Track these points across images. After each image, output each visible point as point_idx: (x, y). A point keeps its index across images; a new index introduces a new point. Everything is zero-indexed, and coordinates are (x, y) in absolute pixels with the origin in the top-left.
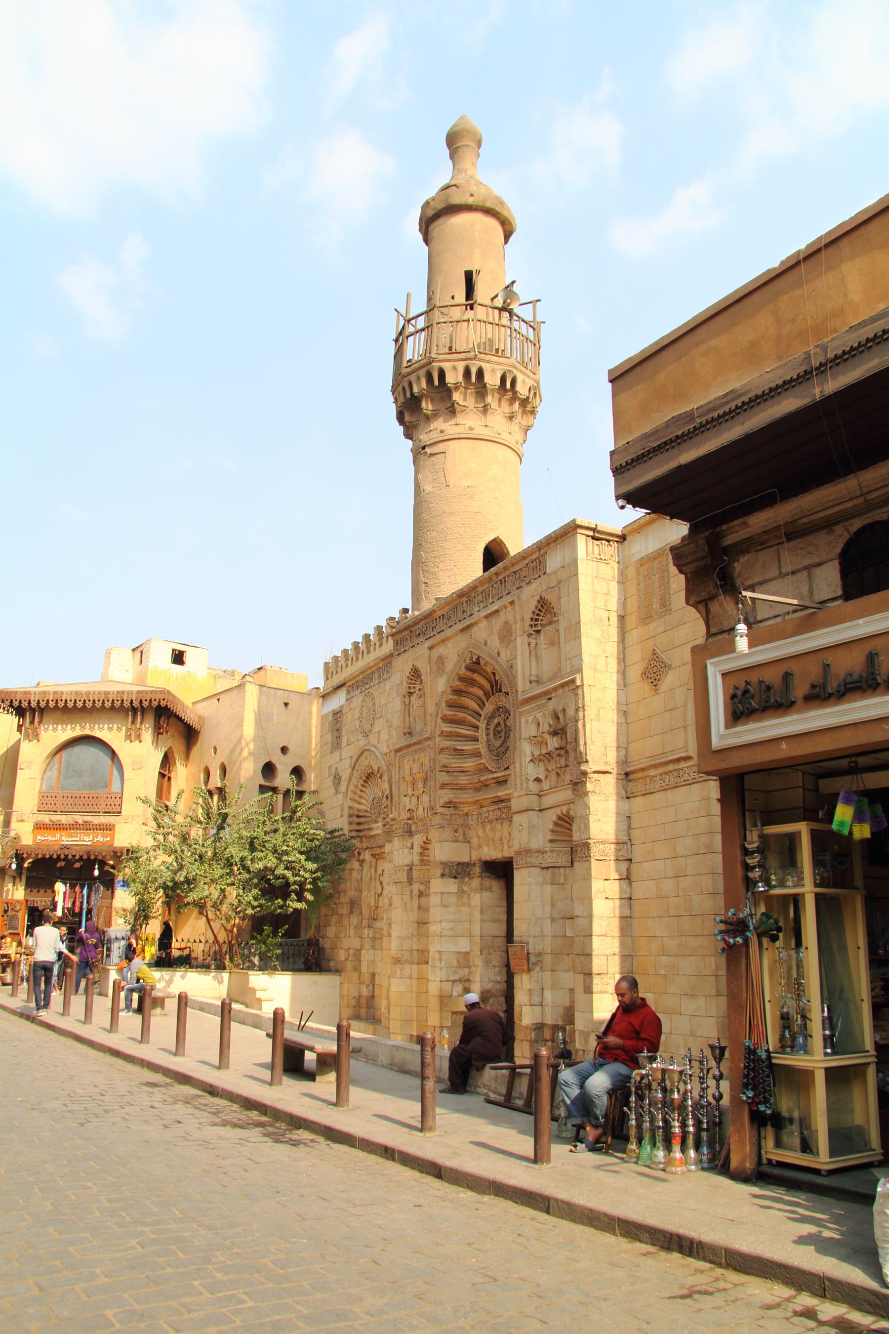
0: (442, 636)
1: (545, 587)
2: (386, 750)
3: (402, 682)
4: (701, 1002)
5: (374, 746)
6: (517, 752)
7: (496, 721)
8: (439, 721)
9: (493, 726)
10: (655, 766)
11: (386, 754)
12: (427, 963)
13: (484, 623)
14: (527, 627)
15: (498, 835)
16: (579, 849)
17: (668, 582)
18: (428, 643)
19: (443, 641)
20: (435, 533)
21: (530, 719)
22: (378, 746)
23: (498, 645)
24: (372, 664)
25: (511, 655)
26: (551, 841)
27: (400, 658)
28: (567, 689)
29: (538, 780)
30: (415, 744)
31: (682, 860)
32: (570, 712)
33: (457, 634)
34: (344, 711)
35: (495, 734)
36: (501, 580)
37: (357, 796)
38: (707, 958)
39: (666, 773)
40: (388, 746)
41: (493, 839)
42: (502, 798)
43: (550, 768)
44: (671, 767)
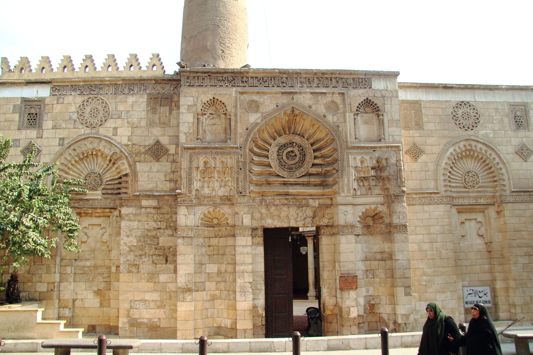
0: (256, 89)
1: (371, 95)
2: (125, 141)
3: (195, 105)
4: (449, 294)
5: (105, 136)
6: (345, 173)
7: (290, 149)
8: (250, 139)
9: (285, 152)
10: (416, 194)
11: (127, 145)
12: (205, 290)
13: (309, 96)
14: (354, 109)
15: (283, 214)
16: (398, 227)
17: (422, 116)
18: (240, 89)
19: (258, 93)
20: (230, 24)
21: (358, 158)
22: (113, 137)
23: (324, 111)
24: (107, 79)
25: (338, 120)
26: (359, 221)
27: (194, 90)
28: (390, 149)
29: (355, 189)
30: (217, 148)
31: (435, 235)
32: (393, 160)
33: (276, 93)
34: (47, 101)
35: (287, 157)
36: (327, 78)
37: (66, 168)
38: (451, 276)
39: (423, 198)
40: (129, 140)
41: (279, 217)
42: (290, 193)
43: (361, 184)
44: (426, 195)
